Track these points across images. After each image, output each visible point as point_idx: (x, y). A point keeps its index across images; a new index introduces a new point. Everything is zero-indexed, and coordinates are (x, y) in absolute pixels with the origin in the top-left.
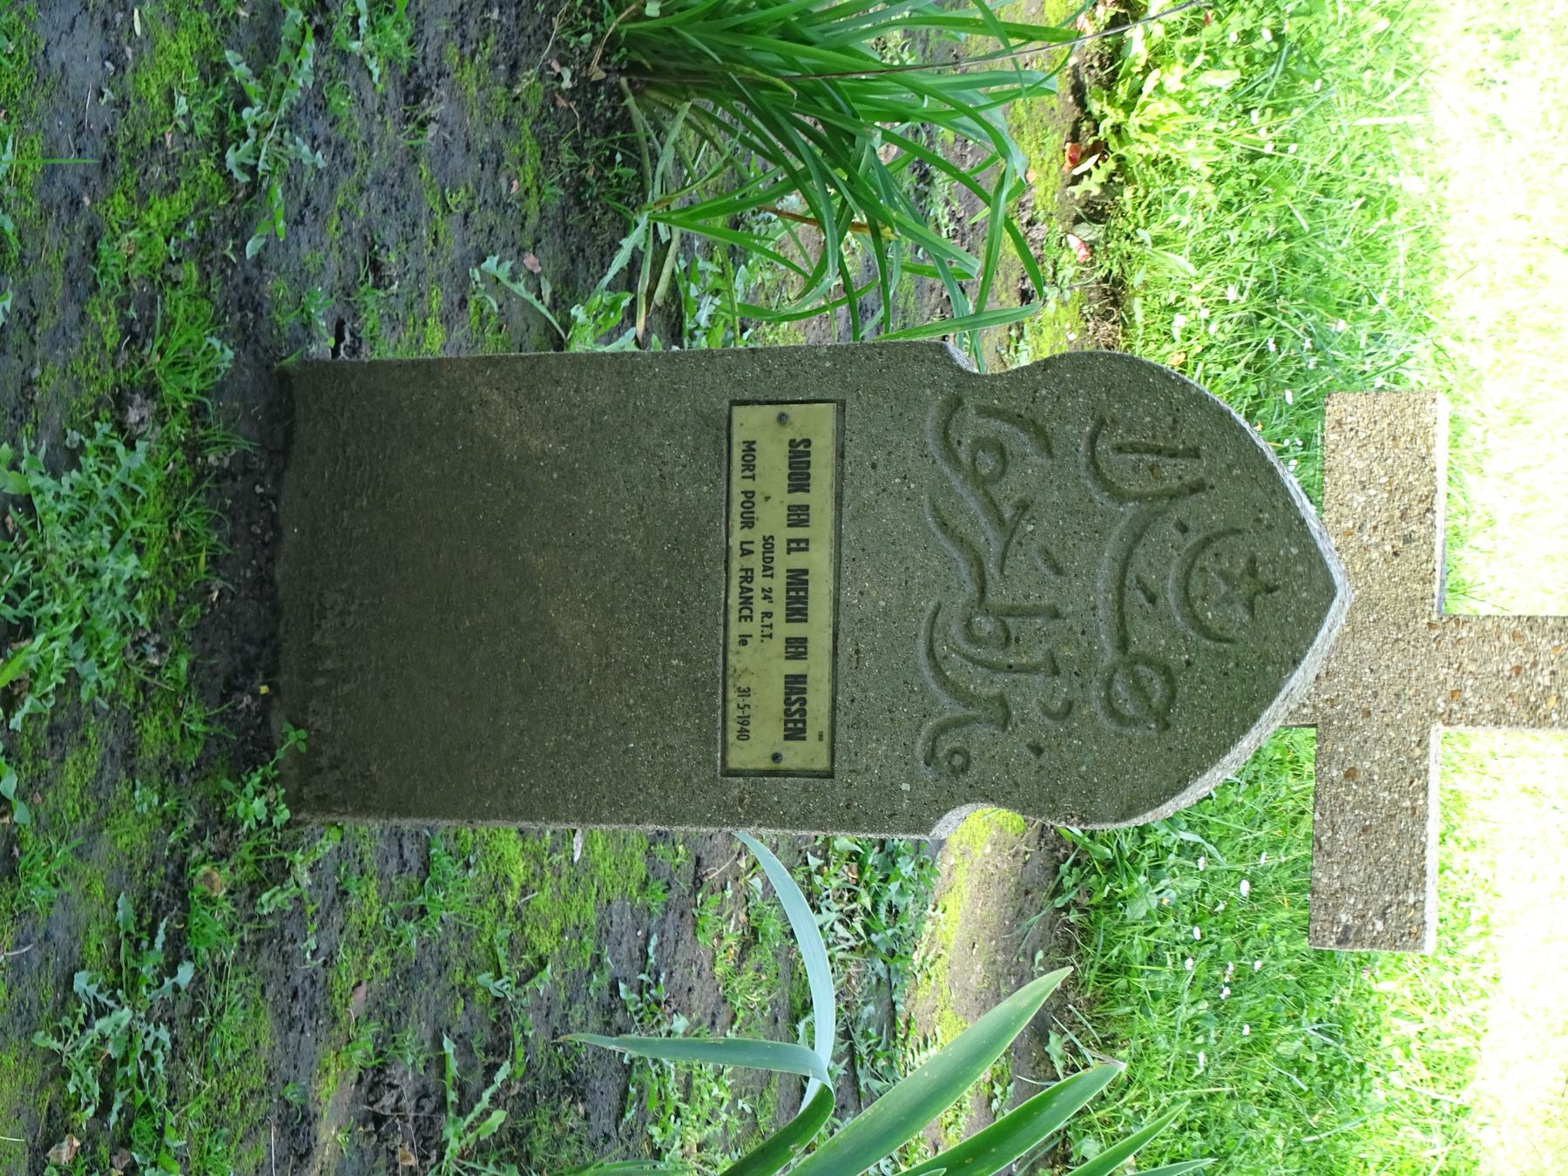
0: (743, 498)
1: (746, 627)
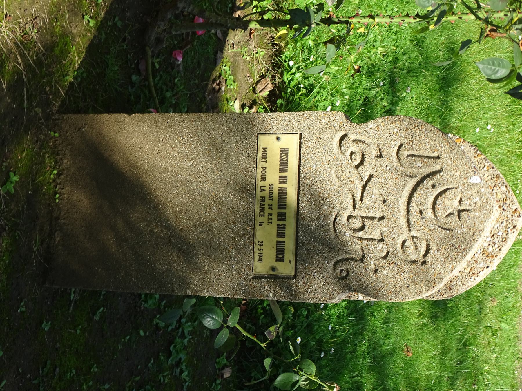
0: (262, 169)
1: (261, 219)
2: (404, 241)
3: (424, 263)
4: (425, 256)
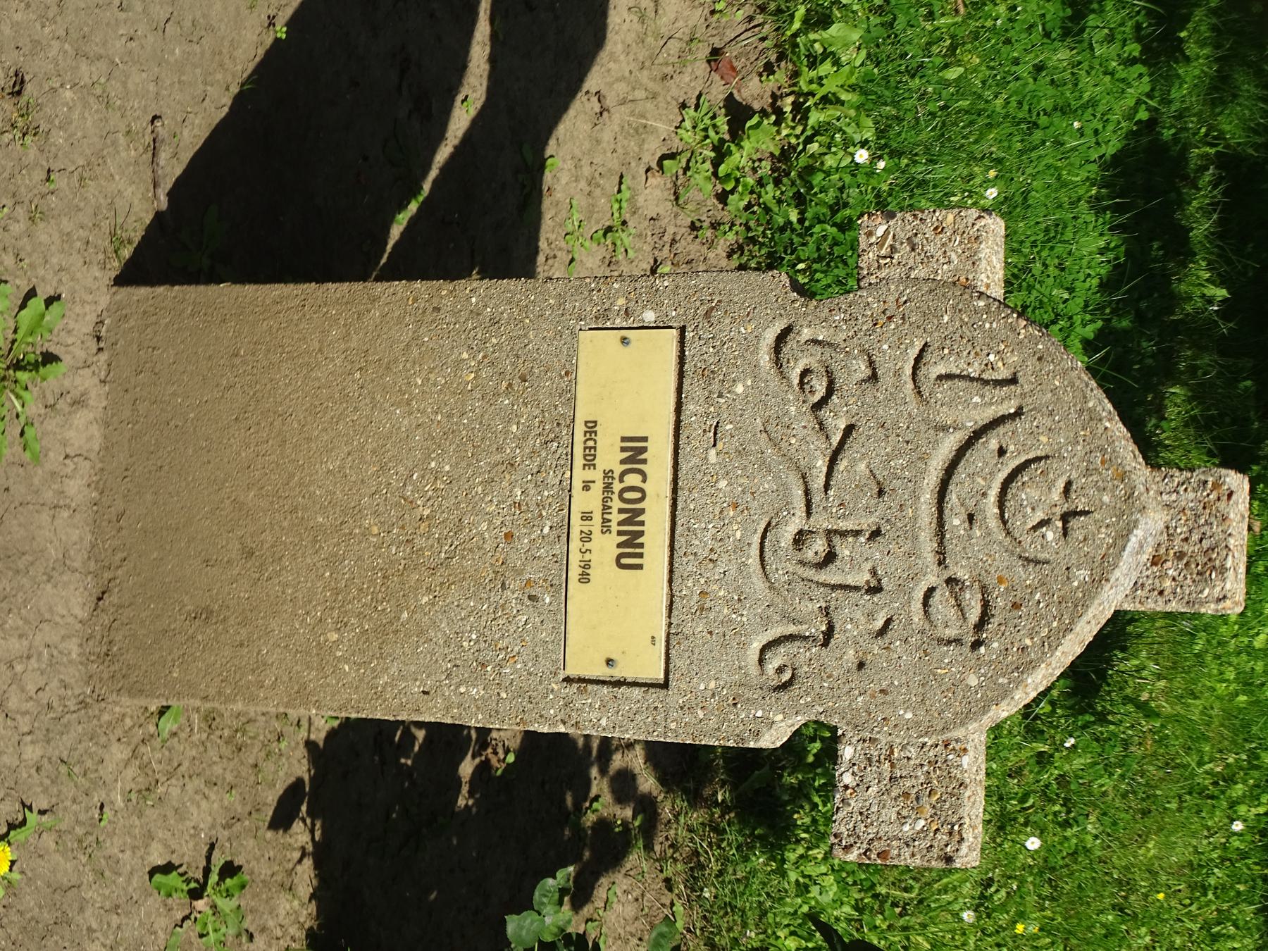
2: (930, 592)
3: (976, 645)
4: (980, 626)
